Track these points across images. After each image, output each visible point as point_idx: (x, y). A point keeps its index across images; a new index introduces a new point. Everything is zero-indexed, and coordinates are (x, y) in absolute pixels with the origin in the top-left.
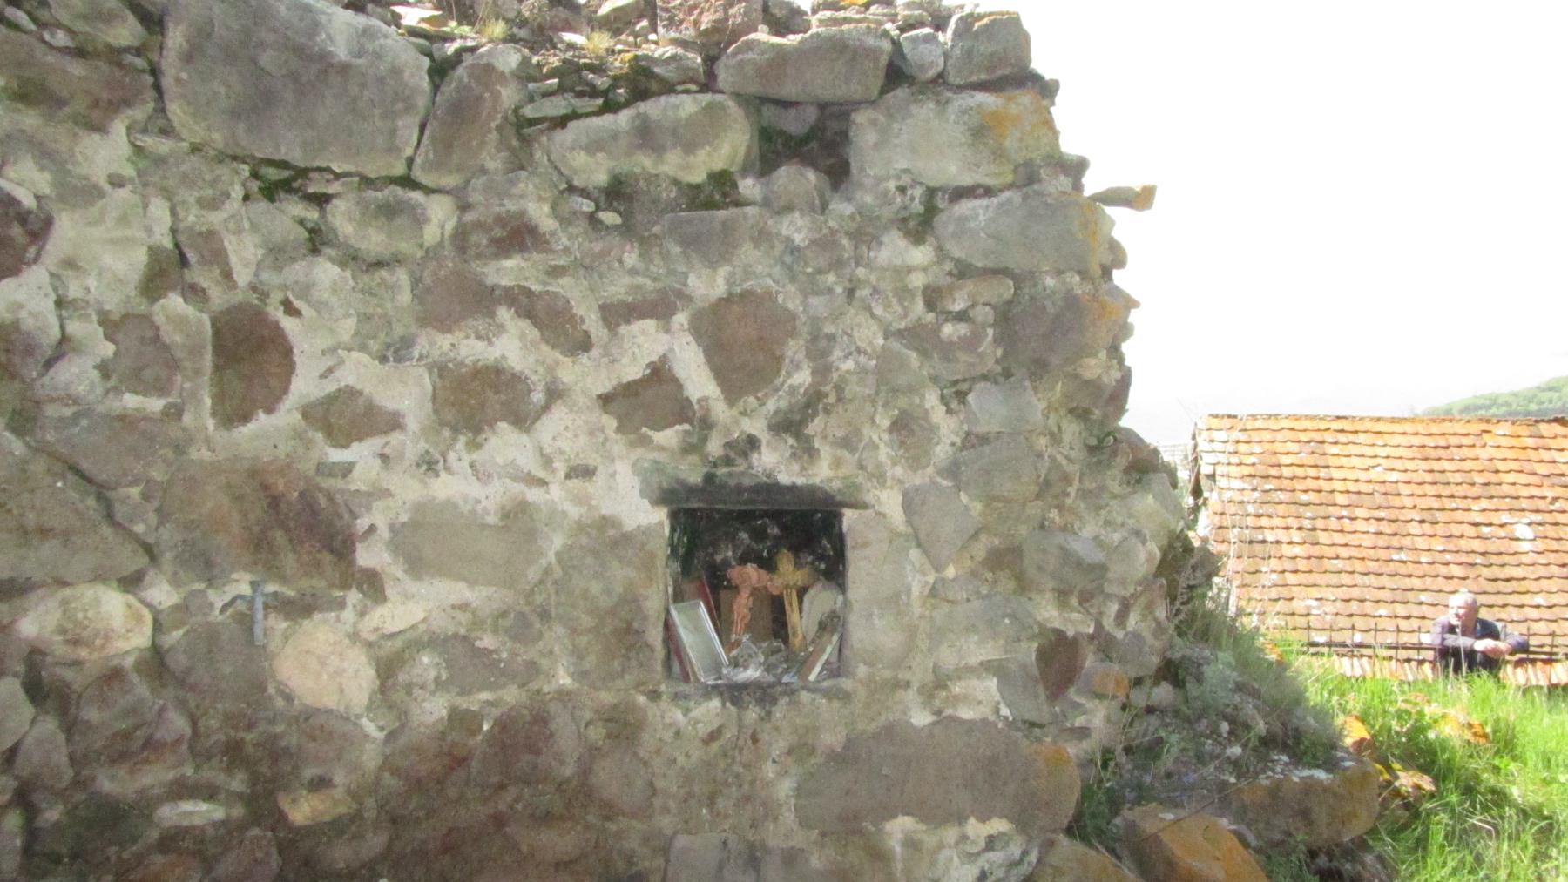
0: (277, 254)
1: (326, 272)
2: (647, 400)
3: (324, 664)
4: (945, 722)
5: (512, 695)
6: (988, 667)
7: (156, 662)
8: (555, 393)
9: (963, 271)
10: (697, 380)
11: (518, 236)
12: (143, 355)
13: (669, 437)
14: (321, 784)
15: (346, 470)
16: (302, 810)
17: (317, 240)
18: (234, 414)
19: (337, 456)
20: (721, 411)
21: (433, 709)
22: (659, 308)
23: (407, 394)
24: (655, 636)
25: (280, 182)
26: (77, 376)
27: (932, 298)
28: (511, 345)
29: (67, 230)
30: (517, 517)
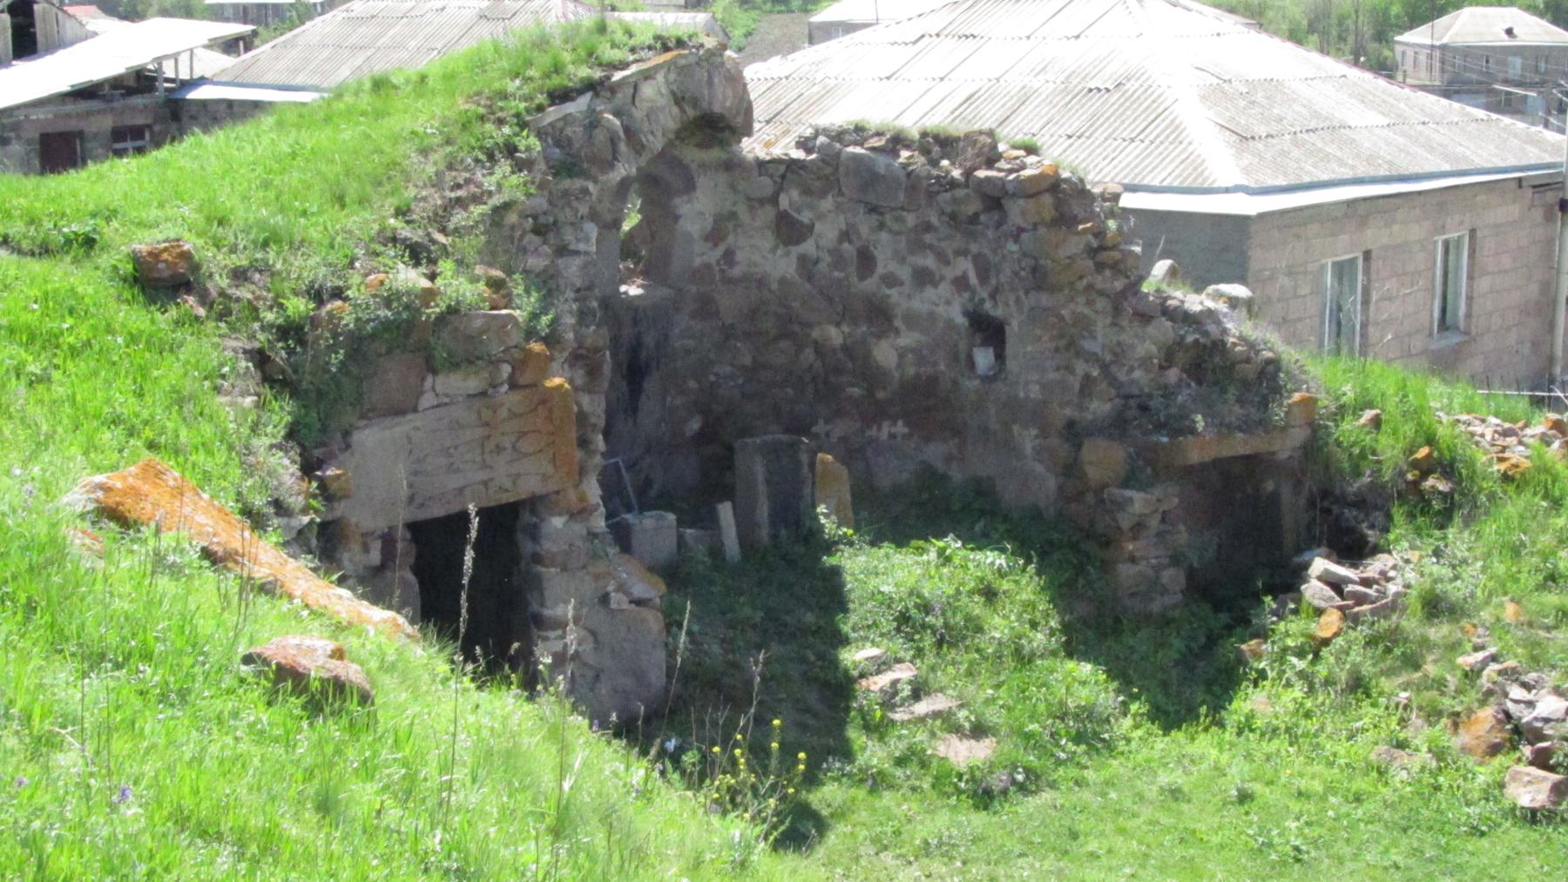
0: (873, 230)
1: (884, 236)
2: (961, 283)
3: (885, 353)
4: (1027, 397)
5: (930, 370)
6: (1037, 382)
7: (845, 348)
8: (942, 278)
9: (1025, 255)
10: (973, 279)
11: (928, 227)
12: (838, 260)
13: (966, 295)
14: (884, 388)
15: (889, 296)
16: (881, 395)
17: (882, 226)
18: (862, 278)
19: (888, 292)
20: (978, 289)
21: (911, 371)
22: (963, 253)
23: (904, 273)
24: (963, 356)
25: (873, 209)
26: (822, 266)
27: (1019, 261)
28: (929, 261)
29: (818, 226)
30: (932, 316)
